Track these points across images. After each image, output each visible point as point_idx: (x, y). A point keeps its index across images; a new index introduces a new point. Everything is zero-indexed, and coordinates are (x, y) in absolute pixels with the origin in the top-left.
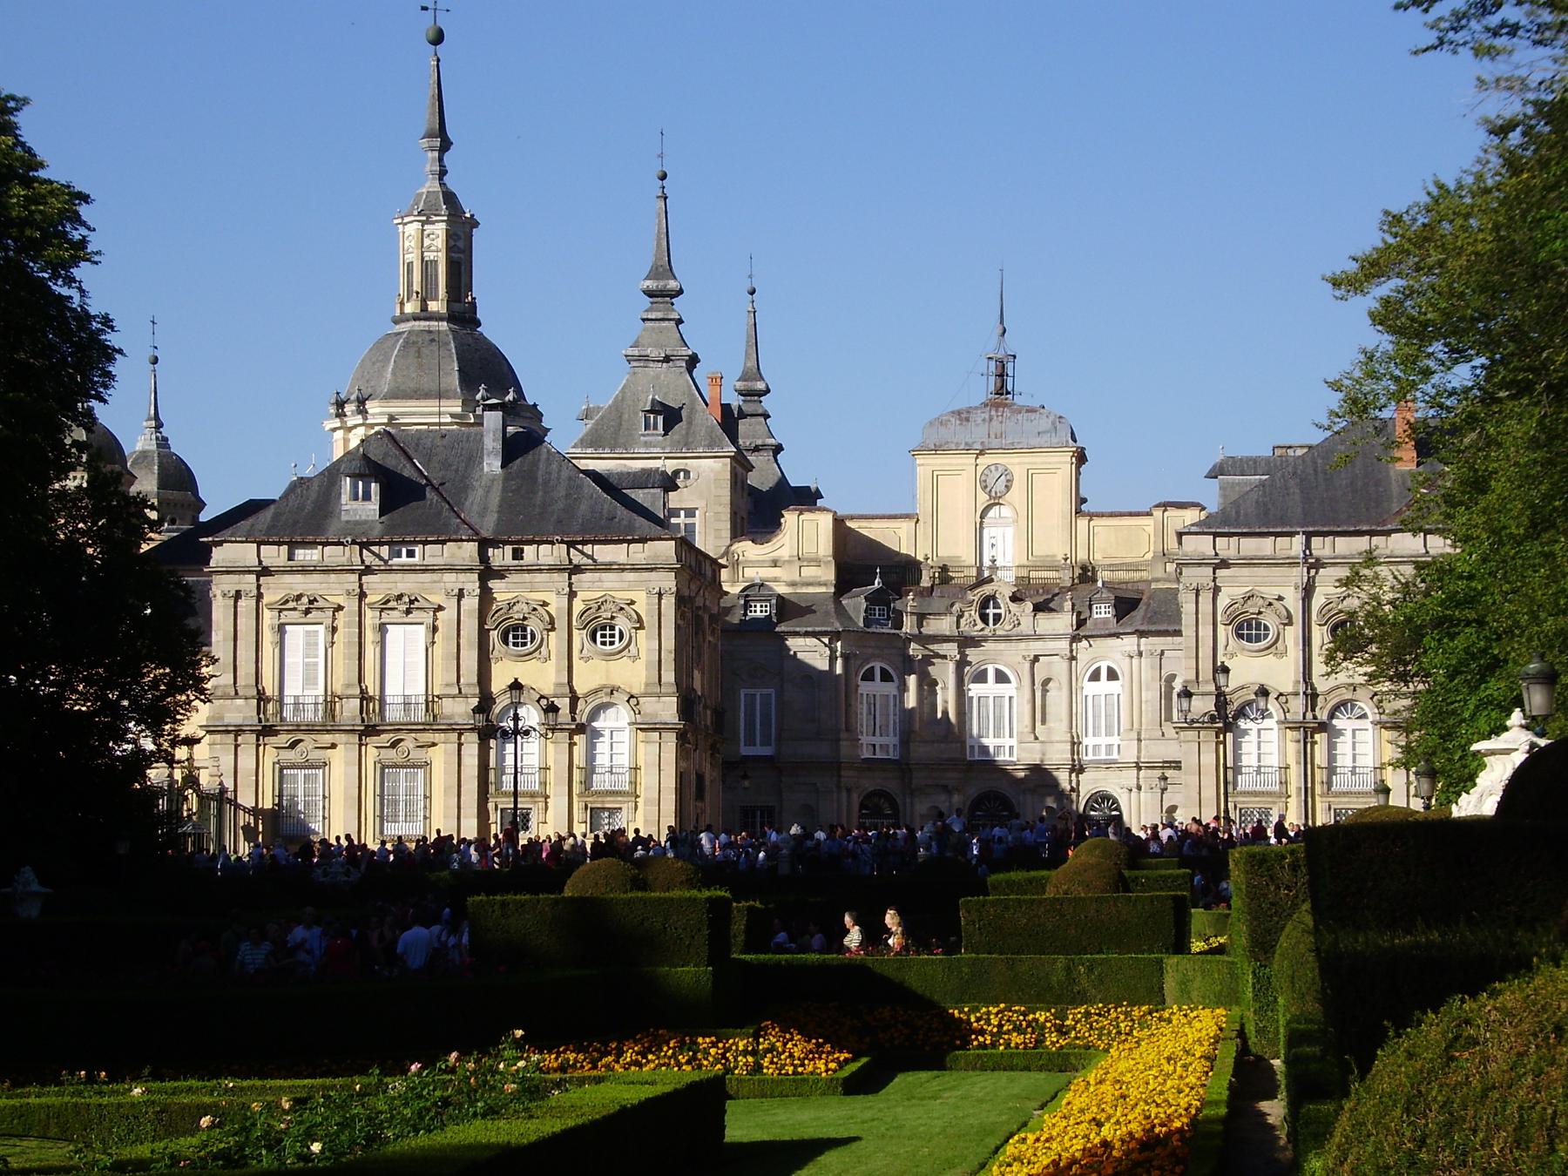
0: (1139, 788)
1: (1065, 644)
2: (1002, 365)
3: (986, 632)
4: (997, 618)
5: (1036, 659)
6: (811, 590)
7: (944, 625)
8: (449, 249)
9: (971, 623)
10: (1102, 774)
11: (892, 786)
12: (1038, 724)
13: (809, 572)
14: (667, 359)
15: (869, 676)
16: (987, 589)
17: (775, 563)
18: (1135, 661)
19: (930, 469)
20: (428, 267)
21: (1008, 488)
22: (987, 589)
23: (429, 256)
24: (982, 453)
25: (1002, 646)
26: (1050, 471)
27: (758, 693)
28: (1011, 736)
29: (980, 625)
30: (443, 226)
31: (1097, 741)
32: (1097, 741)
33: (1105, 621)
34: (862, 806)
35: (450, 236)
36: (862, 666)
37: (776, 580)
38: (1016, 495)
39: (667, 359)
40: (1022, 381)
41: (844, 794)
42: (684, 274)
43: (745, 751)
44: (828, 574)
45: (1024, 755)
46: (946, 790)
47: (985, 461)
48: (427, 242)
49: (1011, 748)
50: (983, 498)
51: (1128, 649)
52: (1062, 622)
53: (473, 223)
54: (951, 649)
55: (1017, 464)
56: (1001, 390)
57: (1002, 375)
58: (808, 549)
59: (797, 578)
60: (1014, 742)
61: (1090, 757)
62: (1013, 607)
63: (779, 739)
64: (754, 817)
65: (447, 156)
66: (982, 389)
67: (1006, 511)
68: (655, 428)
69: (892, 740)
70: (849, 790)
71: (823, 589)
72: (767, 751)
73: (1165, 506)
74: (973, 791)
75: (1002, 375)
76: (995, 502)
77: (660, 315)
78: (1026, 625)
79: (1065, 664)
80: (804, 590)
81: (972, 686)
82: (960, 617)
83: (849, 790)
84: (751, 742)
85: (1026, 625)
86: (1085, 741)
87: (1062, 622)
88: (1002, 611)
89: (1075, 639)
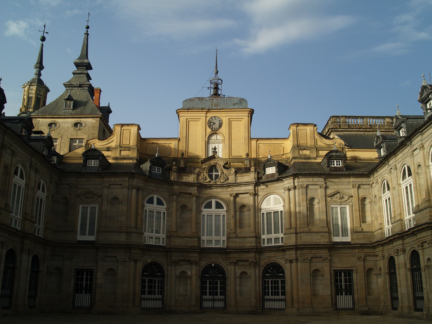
0: (297, 260)
1: (251, 188)
2: (217, 85)
3: (212, 183)
4: (217, 176)
5: (237, 195)
6: (125, 161)
7: (191, 178)
8: (37, 94)
9: (205, 179)
10: (272, 254)
11: (161, 260)
12: (238, 229)
13: (124, 153)
14: (80, 86)
15: (151, 201)
16: (212, 162)
17: (108, 149)
18: (292, 192)
19: (185, 118)
20: (29, 98)
21: (220, 126)
22: (212, 162)
23: (31, 95)
24: (209, 111)
25: (219, 190)
26: (239, 120)
28: (223, 235)
29: (209, 180)
30: (35, 86)
31: (270, 236)
32: (270, 236)
33: (273, 175)
34: (144, 270)
35: (37, 90)
36: (147, 195)
37: (108, 156)
38: (224, 129)
39: (80, 86)
40: (224, 90)
41: (132, 264)
42: (92, 59)
43: (80, 238)
44: (134, 154)
45: (231, 245)
46: (190, 262)
47: (210, 115)
48: (30, 91)
49: (224, 241)
50: (209, 130)
51: (287, 186)
52: (251, 177)
53: (47, 90)
54: (194, 190)
55: (224, 117)
56: (216, 94)
57: (216, 88)
58: (125, 142)
59: (118, 155)
60: (225, 238)
61: (266, 245)
62: (225, 171)
63: (98, 232)
64: (82, 275)
65: (42, 72)
66: (207, 93)
67: (219, 137)
68: (70, 106)
69: (162, 235)
70: (136, 261)
71: (131, 161)
72: (92, 238)
73: (298, 125)
74: (204, 263)
75: (216, 88)
76: (214, 132)
77: (80, 72)
78: (232, 179)
79: (252, 198)
80: (122, 161)
81: (203, 210)
82: (198, 175)
83: (136, 261)
84: (83, 233)
85: (232, 179)
86: (263, 237)
87: (251, 177)
88: (219, 173)
89: (257, 183)
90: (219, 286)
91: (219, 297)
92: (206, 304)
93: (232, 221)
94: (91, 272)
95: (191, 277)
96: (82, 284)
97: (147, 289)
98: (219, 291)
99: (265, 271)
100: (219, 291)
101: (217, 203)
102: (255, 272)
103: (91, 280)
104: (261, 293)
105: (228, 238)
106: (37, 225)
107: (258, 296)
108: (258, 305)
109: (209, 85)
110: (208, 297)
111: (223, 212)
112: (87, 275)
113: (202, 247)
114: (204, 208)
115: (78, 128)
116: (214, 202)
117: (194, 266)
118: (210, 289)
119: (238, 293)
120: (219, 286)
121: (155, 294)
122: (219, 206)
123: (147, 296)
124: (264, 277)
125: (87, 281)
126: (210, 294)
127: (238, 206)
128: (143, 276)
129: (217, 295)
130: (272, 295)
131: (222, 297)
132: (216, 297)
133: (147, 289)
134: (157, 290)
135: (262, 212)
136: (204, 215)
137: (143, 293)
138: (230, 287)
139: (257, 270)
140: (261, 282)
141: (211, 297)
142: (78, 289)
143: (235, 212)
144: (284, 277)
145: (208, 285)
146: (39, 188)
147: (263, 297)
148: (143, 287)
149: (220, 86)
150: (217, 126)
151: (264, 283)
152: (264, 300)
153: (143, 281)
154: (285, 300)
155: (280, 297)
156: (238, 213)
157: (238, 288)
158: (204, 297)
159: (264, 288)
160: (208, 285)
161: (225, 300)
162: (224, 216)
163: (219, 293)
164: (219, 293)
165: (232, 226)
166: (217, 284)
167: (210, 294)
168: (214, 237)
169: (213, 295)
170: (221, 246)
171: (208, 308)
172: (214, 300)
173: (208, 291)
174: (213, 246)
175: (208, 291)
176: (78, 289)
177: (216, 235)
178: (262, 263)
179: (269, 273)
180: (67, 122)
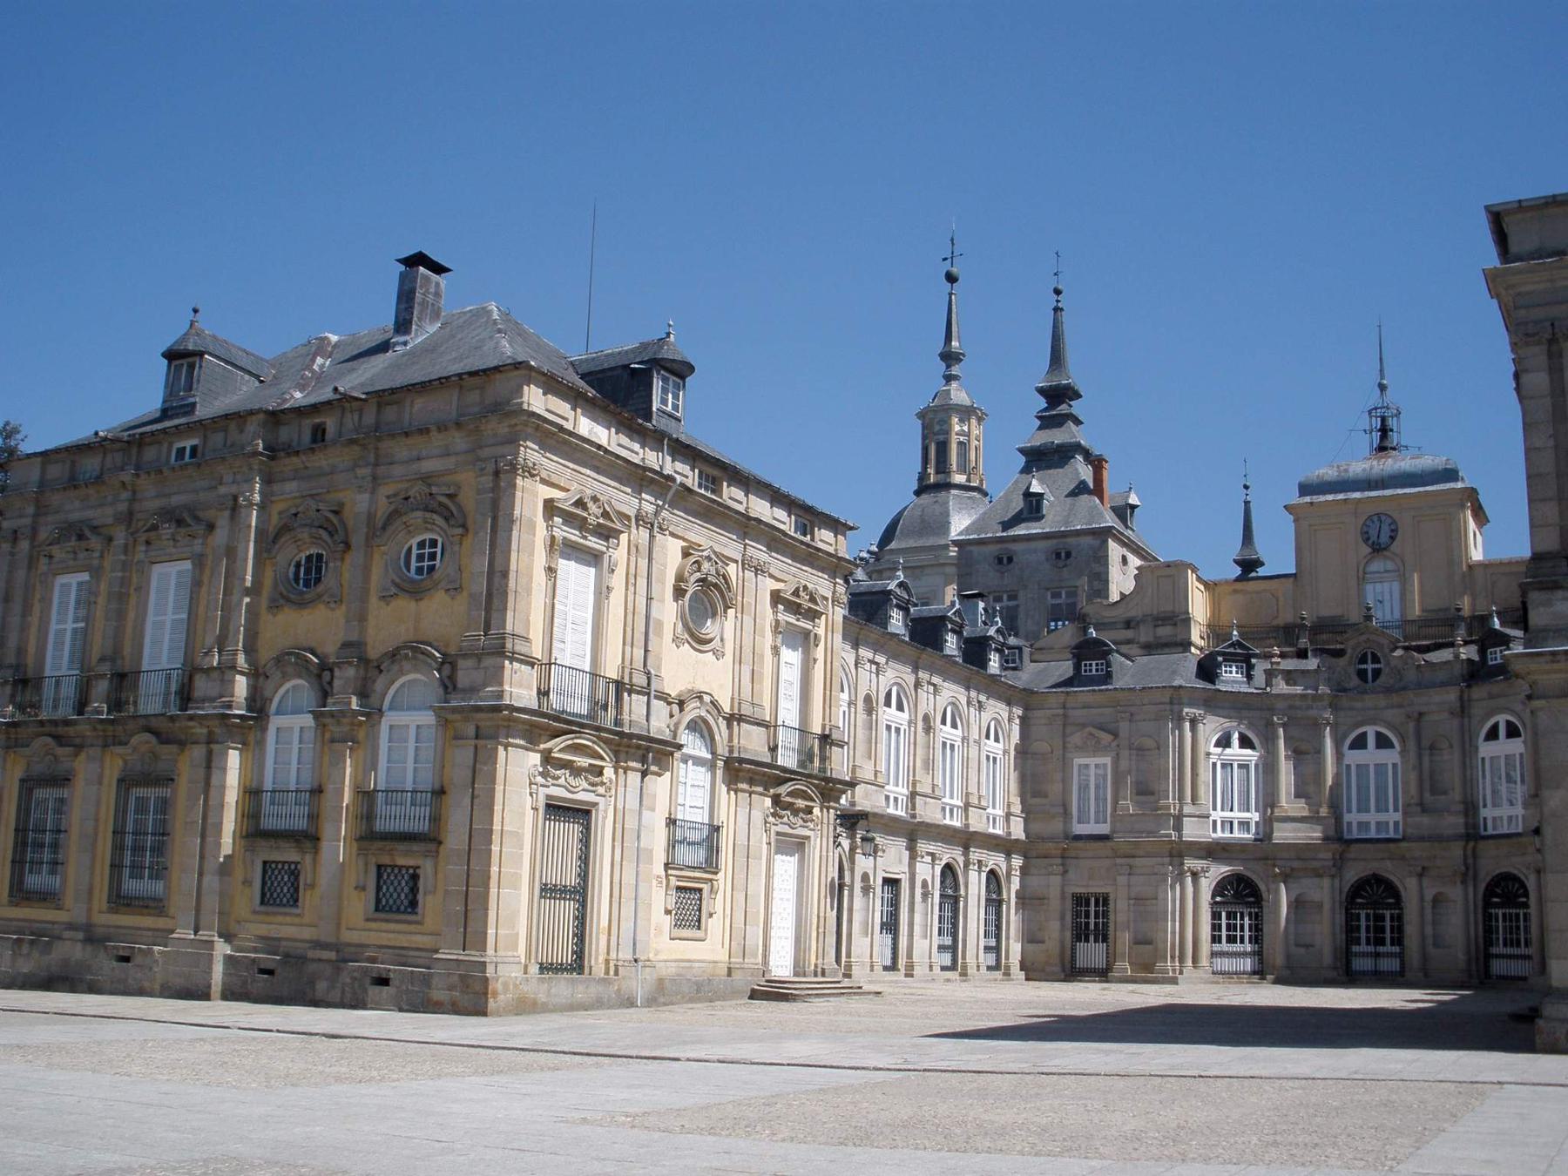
12: (1427, 795)
21: (1393, 538)
27: (1092, 761)
28: (1396, 810)
45: (1409, 831)
49: (1396, 824)
57: (1384, 431)
59: (1151, 639)
60: (1398, 816)
64: (1088, 904)
72: (1104, 829)
74: (1352, 874)
75: (1384, 431)
90: (1388, 924)
91: (1388, 948)
92: (1360, 964)
93: (1413, 776)
94: (1103, 900)
95: (1320, 906)
96: (1087, 924)
97: (1224, 933)
98: (1388, 935)
99: (1490, 891)
100: (1388, 935)
101: (1379, 735)
102: (1466, 894)
103: (1105, 914)
104: (1481, 941)
105: (1405, 813)
106: (990, 810)
107: (1473, 948)
108: (1474, 968)
109: (1365, 422)
110: (1363, 948)
111: (1390, 757)
112: (1097, 904)
113: (1346, 836)
114: (1352, 747)
115: (1061, 564)
116: (1371, 731)
117: (1326, 882)
118: (1368, 930)
119: (1430, 941)
120: (1388, 924)
121: (1242, 942)
122: (1383, 742)
123: (1224, 946)
124: (1487, 904)
125: (1097, 917)
126: (1368, 943)
127: (1426, 743)
128: (1214, 904)
129: (1382, 942)
130: (1505, 945)
131: (1396, 949)
132: (1381, 949)
133: (1224, 933)
134: (1247, 933)
135: (1481, 755)
136: (1348, 766)
137: (1216, 939)
138: (1411, 929)
139: (1471, 889)
140: (1480, 917)
141: (1371, 949)
142: (1081, 934)
143: (1420, 756)
144: (1526, 905)
145: (1363, 923)
146: (988, 737)
147: (1486, 949)
148: (1216, 927)
149: (1392, 423)
150: (1384, 539)
151: (1488, 917)
152: (1488, 957)
153: (1216, 916)
154: (1528, 957)
155: (1522, 950)
156: (1426, 760)
157: (1429, 930)
158: (1355, 949)
159: (1489, 931)
160: (1363, 923)
161: (1401, 956)
162: (1395, 765)
163: (1388, 941)
164: (1388, 941)
165: (1413, 790)
166: (1382, 918)
167: (1368, 943)
168: (1372, 817)
169: (1376, 944)
170: (1391, 835)
171: (1364, 973)
172: (1377, 955)
173: (1363, 935)
174: (1373, 834)
175: (1363, 935)
176: (1081, 934)
177: (1378, 810)
178: (1482, 874)
179: (1497, 896)
180: (1035, 551)
